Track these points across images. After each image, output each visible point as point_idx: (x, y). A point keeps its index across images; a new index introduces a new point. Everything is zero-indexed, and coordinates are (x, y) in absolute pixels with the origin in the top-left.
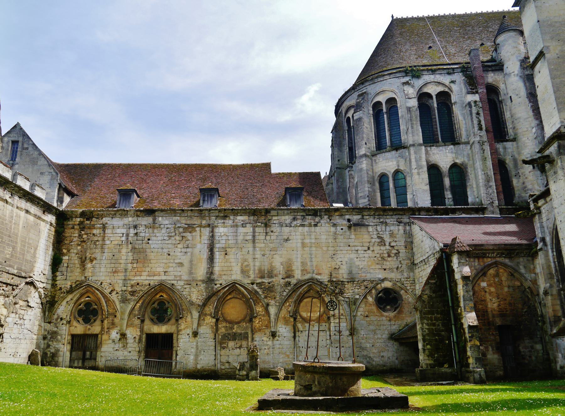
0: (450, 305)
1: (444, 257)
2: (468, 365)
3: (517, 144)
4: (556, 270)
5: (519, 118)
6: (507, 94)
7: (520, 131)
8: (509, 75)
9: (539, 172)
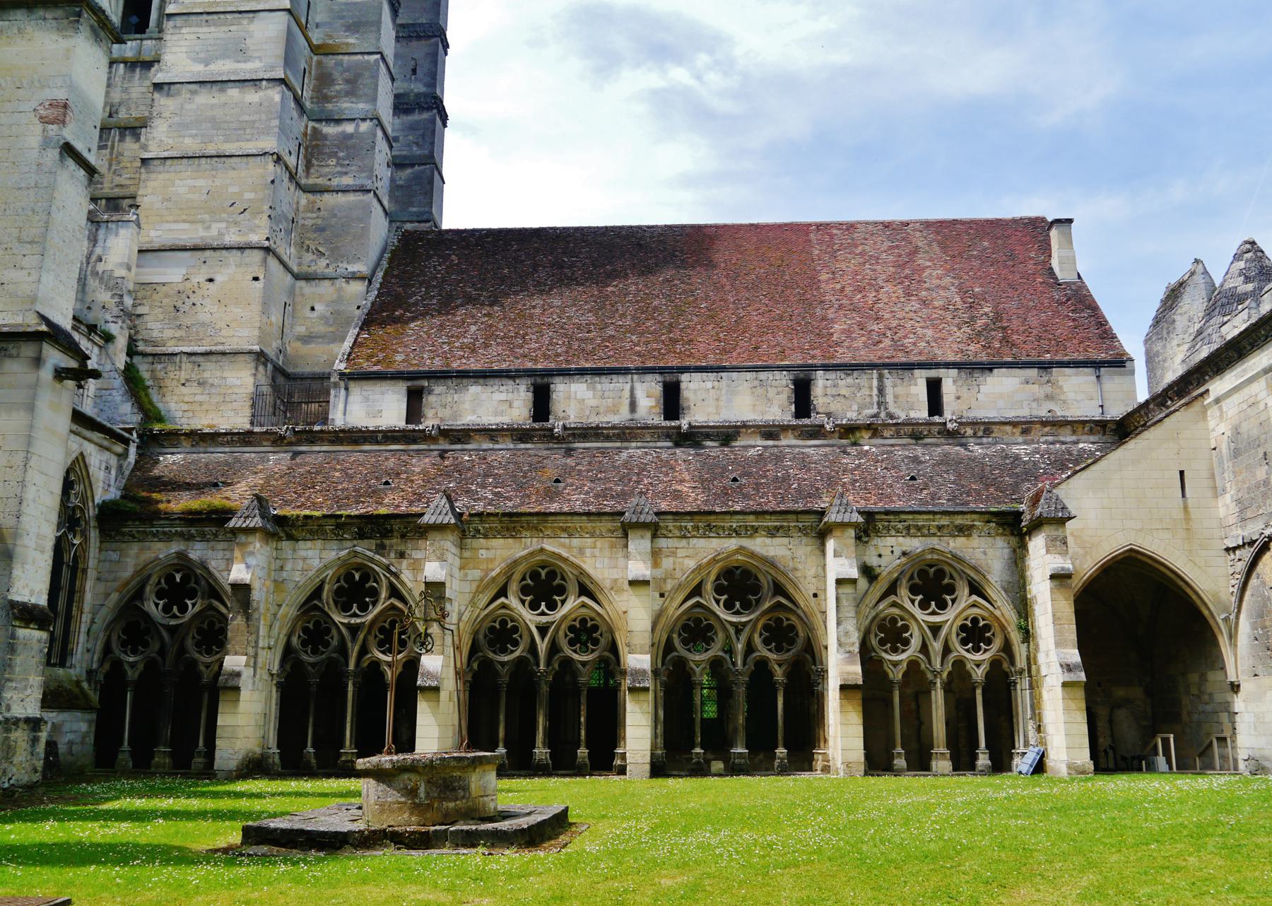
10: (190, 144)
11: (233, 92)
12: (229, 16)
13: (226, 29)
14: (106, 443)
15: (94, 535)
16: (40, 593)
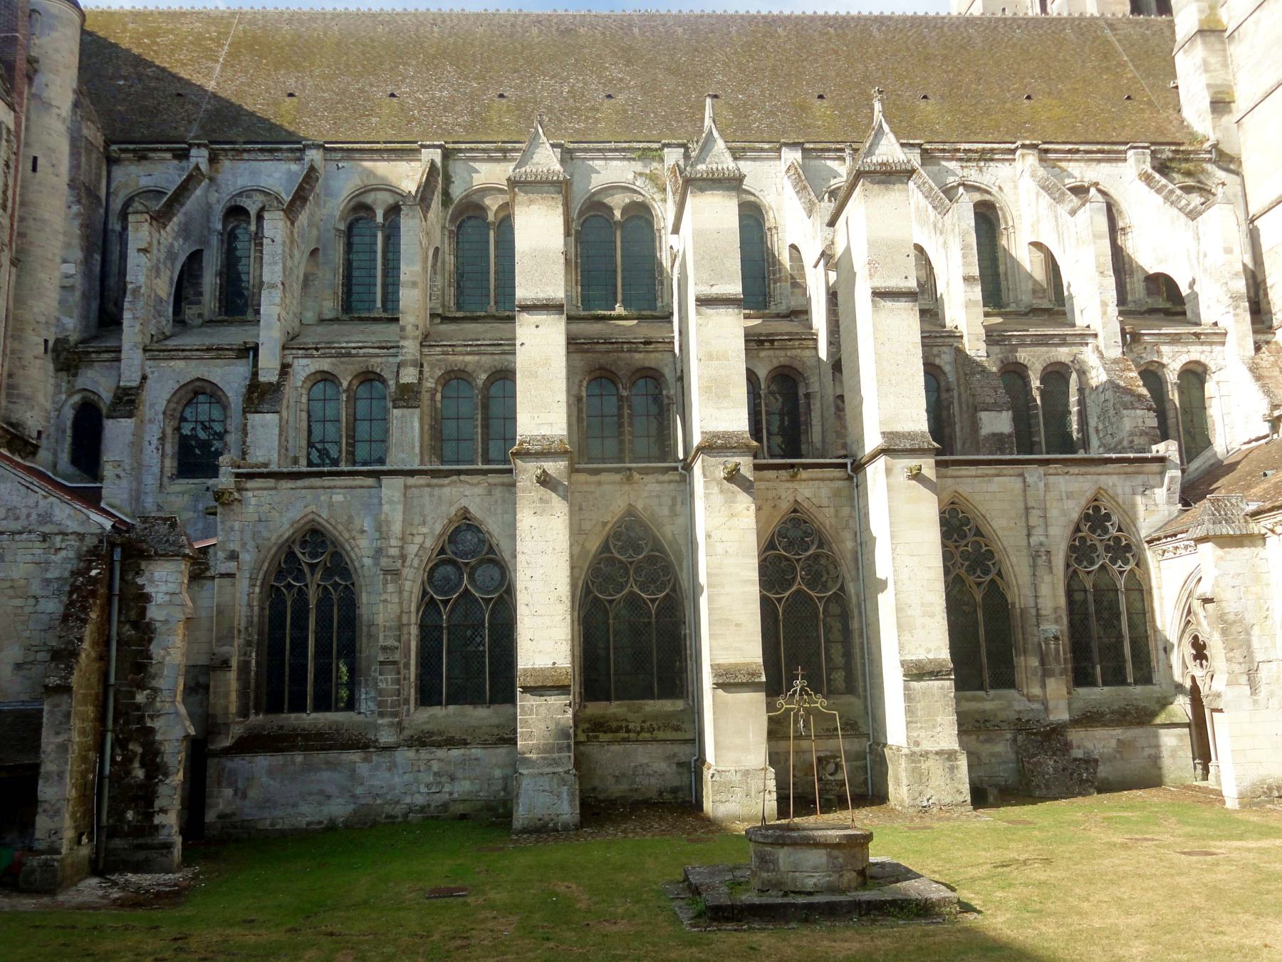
4: (250, 623)
9: (51, 366)
16: (939, 648)
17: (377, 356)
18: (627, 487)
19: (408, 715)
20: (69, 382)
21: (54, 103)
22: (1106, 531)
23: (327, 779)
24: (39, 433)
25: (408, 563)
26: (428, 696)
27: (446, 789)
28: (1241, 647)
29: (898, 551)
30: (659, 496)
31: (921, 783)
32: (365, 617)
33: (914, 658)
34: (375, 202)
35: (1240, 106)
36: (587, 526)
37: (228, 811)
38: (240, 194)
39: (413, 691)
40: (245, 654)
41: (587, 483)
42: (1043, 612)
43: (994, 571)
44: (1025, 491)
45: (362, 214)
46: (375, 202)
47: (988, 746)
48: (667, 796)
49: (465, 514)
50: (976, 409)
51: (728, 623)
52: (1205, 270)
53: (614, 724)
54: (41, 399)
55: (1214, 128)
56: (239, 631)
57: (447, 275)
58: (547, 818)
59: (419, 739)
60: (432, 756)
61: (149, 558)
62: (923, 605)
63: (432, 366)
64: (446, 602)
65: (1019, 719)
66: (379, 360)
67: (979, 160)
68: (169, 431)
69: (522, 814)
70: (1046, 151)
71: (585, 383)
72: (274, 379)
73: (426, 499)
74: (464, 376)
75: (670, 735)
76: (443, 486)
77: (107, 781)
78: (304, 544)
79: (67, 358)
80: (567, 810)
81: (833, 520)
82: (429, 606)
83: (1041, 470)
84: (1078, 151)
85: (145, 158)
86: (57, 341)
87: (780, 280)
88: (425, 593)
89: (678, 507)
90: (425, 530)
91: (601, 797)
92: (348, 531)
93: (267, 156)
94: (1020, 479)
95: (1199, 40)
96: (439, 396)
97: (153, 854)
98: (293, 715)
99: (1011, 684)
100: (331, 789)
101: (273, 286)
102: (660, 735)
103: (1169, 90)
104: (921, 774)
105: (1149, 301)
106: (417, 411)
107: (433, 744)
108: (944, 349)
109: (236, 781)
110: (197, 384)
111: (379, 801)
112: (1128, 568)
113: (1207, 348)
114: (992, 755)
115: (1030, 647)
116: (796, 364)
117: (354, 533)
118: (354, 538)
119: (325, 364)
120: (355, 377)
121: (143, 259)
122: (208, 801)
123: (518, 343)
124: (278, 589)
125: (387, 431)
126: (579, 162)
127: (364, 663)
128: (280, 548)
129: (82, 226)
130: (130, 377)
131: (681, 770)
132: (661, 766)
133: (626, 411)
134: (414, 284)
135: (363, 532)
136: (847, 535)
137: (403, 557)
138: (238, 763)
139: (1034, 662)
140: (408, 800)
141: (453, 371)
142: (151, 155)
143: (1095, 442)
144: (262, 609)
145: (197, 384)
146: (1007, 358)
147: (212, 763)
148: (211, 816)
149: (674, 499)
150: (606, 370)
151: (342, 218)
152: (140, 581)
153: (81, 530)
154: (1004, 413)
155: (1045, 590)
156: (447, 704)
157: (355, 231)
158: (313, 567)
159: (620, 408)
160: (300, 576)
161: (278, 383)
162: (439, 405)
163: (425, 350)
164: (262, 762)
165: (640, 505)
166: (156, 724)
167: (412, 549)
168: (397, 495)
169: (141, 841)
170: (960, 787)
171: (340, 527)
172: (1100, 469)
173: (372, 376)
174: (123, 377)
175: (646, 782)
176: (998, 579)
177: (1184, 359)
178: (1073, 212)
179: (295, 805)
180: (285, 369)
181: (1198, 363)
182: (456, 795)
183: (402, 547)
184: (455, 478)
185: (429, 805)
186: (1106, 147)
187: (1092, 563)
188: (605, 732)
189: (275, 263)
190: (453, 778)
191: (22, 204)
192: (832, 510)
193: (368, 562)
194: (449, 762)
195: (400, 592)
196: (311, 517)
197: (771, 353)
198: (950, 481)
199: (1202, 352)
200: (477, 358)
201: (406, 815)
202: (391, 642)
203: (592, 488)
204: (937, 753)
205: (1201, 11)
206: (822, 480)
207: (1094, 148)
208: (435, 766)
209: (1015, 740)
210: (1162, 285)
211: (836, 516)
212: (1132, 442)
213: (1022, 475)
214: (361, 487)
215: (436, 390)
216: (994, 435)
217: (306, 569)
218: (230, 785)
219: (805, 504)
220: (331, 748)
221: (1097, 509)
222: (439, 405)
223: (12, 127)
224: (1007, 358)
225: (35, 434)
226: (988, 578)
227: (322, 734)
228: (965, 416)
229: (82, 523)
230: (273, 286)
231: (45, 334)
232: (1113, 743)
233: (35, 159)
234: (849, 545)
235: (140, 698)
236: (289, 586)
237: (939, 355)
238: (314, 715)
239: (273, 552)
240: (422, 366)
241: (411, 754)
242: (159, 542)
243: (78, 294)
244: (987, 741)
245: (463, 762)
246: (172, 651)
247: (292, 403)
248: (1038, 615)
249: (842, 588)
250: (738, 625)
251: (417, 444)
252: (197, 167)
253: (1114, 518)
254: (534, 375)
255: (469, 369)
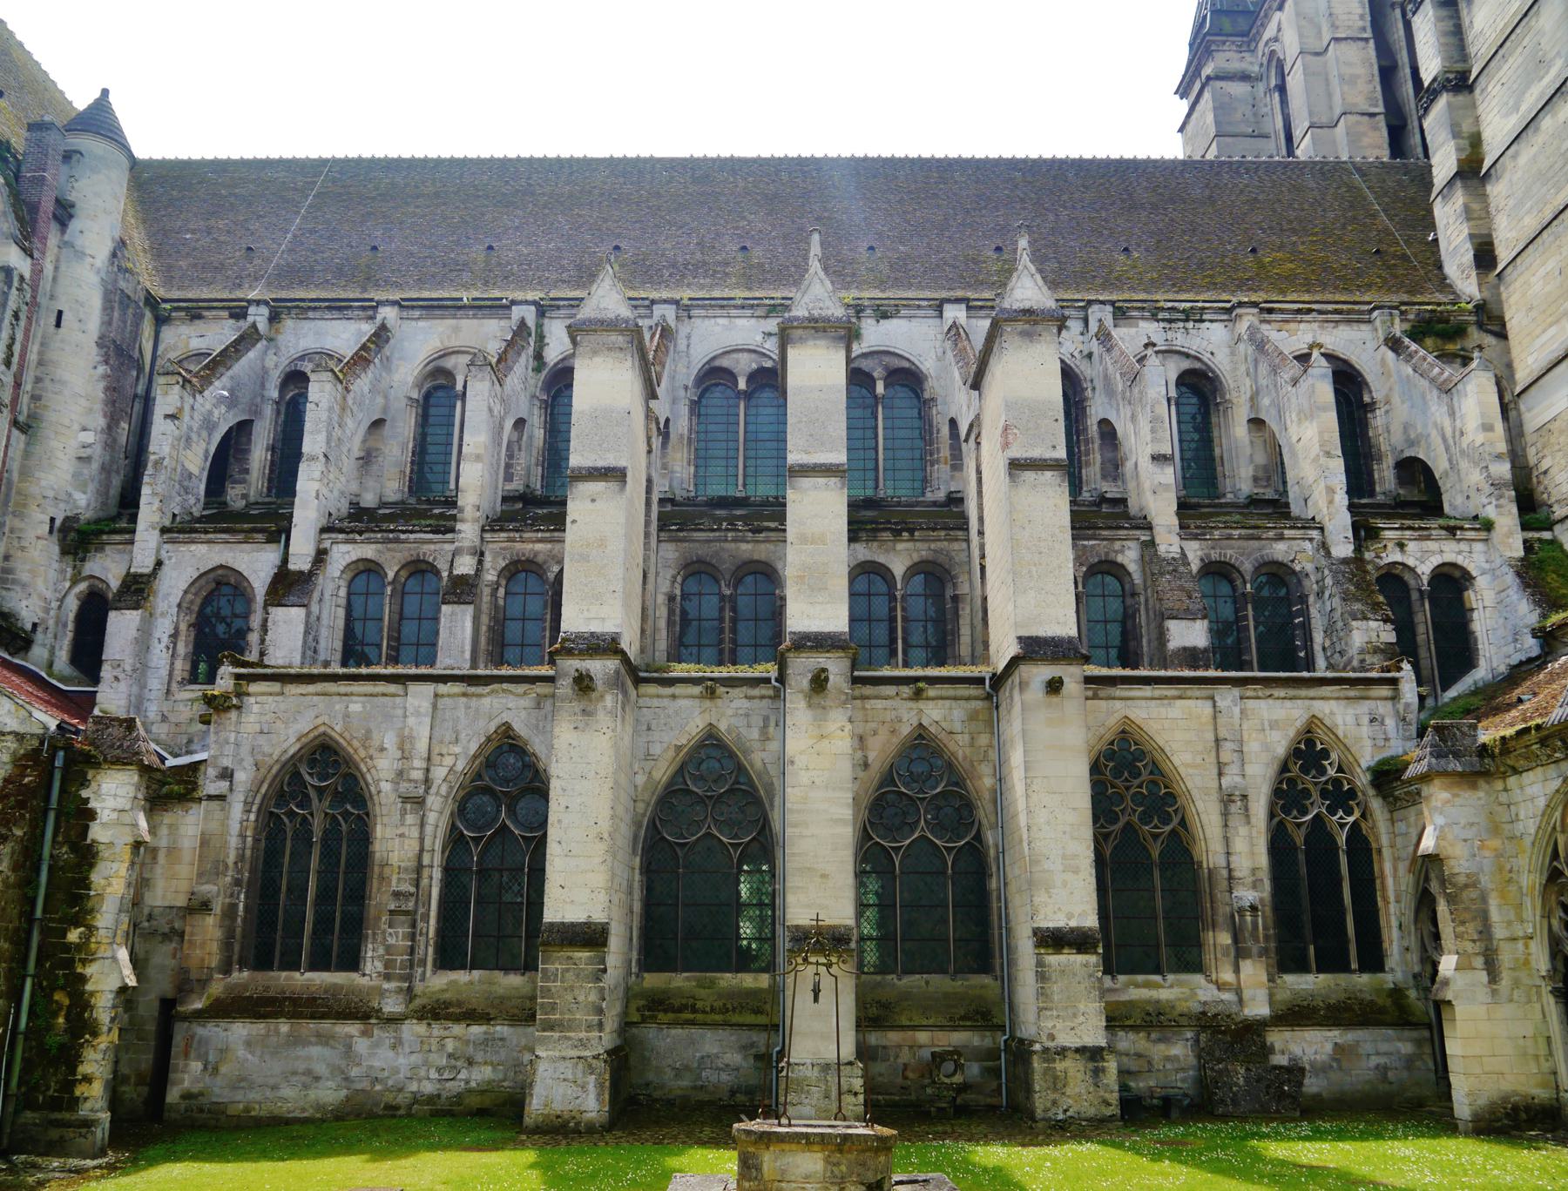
0: (39, 913)
1: (59, 763)
2: (74, 1103)
3: (28, 444)
4: (241, 857)
5: (63, 383)
6: (52, 297)
7: (50, 416)
8: (80, 255)
9: (56, 549)
10: (1531, 223)
11: (1547, 123)
12: (1518, 31)
13: (1520, 49)
14: (1352, 693)
15: (1376, 805)
16: (1083, 915)
17: (431, 542)
18: (708, 703)
19: (423, 979)
20: (75, 567)
21: (88, 251)
22: (1323, 771)
23: (318, 1056)
24: (35, 625)
25: (433, 790)
26: (448, 957)
27: (462, 1076)
28: (1474, 919)
29: (1034, 787)
30: (747, 715)
31: (1055, 1089)
32: (377, 855)
33: (1051, 925)
34: (455, 367)
35: (1503, 254)
36: (656, 749)
37: (195, 1090)
38: (302, 358)
39: (431, 950)
40: (232, 895)
41: (658, 696)
42: (1237, 874)
43: (1176, 820)
44: (1215, 718)
45: (442, 381)
46: (455, 367)
47: (1162, 1047)
48: (740, 1098)
49: (506, 731)
50: (1163, 617)
51: (820, 877)
52: (1462, 452)
53: (677, 1003)
54: (40, 585)
55: (1480, 285)
56: (227, 866)
57: (534, 453)
58: (566, 1116)
59: (433, 1009)
60: (446, 1033)
61: (97, 765)
62: (1064, 857)
63: (496, 555)
64: (477, 840)
65: (1204, 1013)
66: (432, 547)
67: (1187, 320)
68: (183, 627)
69: (536, 1107)
70: (1270, 311)
71: (679, 579)
72: (306, 567)
73: (461, 713)
74: (534, 568)
75: (750, 1018)
76: (480, 696)
77: (21, 1038)
78: (312, 763)
79: (78, 539)
80: (591, 1104)
81: (968, 750)
82: (455, 841)
83: (1236, 692)
84: (1310, 311)
85: (200, 317)
86: (67, 519)
87: (938, 461)
88: (453, 827)
89: (771, 729)
90: (457, 749)
91: (657, 1094)
92: (365, 748)
93: (336, 314)
94: (1209, 703)
95: (1459, 184)
96: (501, 592)
97: (70, 1133)
98: (284, 974)
99: (1197, 967)
100: (320, 1069)
101: (313, 458)
102: (736, 1018)
103: (1428, 243)
104: (1056, 1078)
105: (1401, 492)
106: (470, 608)
107: (448, 1017)
108: (1128, 543)
109: (207, 1053)
110: (220, 572)
111: (378, 1087)
112: (1351, 819)
113: (1464, 546)
114: (1168, 1059)
115: (1220, 919)
116: (941, 559)
117: (372, 751)
118: (371, 758)
119: (369, 551)
120: (402, 567)
121: (169, 426)
122: (172, 1076)
123: (569, 520)
124: (278, 816)
125: (437, 633)
126: (698, 321)
127: (372, 912)
128: (283, 767)
129: (107, 389)
130: (142, 561)
131: (759, 1064)
132: (734, 1058)
133: (728, 614)
134: (478, 458)
135: (382, 749)
136: (985, 769)
137: (427, 781)
138: (213, 1032)
139: (1225, 939)
140: (414, 1087)
141: (519, 561)
142: (206, 313)
143: (1321, 662)
144: (256, 840)
145: (220, 572)
146: (1208, 555)
147: (180, 1031)
148: (173, 1095)
149: (766, 719)
150: (709, 564)
151: (419, 386)
152: (84, 794)
153: (21, 730)
154: (1199, 622)
155: (1239, 845)
156: (472, 968)
157: (432, 401)
158: (320, 791)
159: (722, 610)
160: (305, 802)
161: (310, 571)
162: (501, 602)
163: (487, 536)
164: (240, 1031)
165: (723, 726)
166: (89, 970)
167: (439, 773)
168: (426, 705)
169: (57, 1116)
170: (1107, 1096)
171: (356, 743)
172: (1312, 692)
173: (424, 567)
174: (135, 563)
175: (714, 1078)
176: (1181, 830)
177: (1436, 560)
178: (1295, 382)
179: (275, 1088)
180: (321, 556)
181: (1454, 565)
182: (473, 1084)
183: (428, 770)
184: (495, 686)
185: (439, 1096)
186: (1345, 307)
187: (1305, 813)
188: (666, 1011)
189: (319, 432)
190: (470, 1062)
191: (40, 363)
192: (967, 737)
193: (386, 787)
194: (468, 1042)
195: (422, 825)
196: (322, 729)
197: (910, 545)
198: (1118, 704)
199: (1460, 553)
200: (549, 546)
201: (410, 1107)
202: (407, 887)
203: (666, 702)
204: (1077, 1050)
205: (1459, 149)
206: (955, 698)
207: (1330, 307)
208: (450, 1046)
209: (1197, 1041)
210: (1414, 470)
211: (972, 745)
212: (1363, 661)
213: (1212, 698)
214: (384, 695)
215: (498, 584)
216: (1185, 649)
217: (312, 794)
218: (198, 1058)
219: (932, 729)
220: (323, 1016)
221: (1310, 743)
222: (501, 602)
223: (27, 275)
224: (1208, 555)
225: (28, 627)
226: (1168, 828)
227: (315, 999)
228: (1153, 625)
229: (22, 722)
230: (313, 458)
231: (52, 512)
232: (1329, 1048)
233: (60, 313)
234: (988, 782)
235: (73, 936)
236: (291, 814)
237: (1122, 552)
238: (308, 975)
239: (274, 771)
240: (482, 554)
241: (420, 1028)
242: (112, 746)
243: (95, 466)
244: (1159, 1040)
245: (486, 1042)
246: (114, 881)
247: (327, 596)
248: (1230, 878)
249: (978, 837)
250: (824, 876)
251: (468, 648)
252: (254, 325)
253: (1334, 756)
254: (585, 558)
255: (540, 559)
